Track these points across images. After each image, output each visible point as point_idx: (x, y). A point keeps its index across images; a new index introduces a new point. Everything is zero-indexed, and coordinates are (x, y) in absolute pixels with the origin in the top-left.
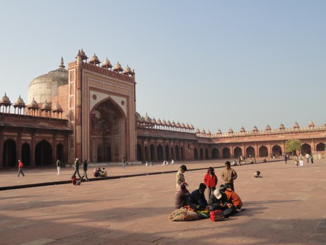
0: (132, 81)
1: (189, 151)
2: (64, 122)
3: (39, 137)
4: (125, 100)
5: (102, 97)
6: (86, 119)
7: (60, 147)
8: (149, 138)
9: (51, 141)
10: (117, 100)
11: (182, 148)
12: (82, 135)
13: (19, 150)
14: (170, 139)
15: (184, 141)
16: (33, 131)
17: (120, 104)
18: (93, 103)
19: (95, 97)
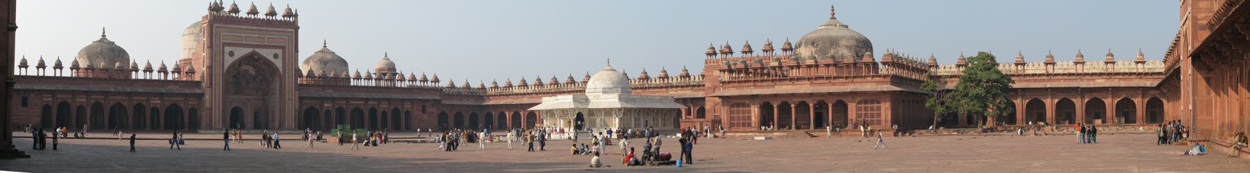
0: (295, 27)
1: (425, 116)
2: (198, 84)
3: (168, 102)
4: (279, 52)
5: (240, 52)
6: (219, 80)
7: (193, 111)
8: (333, 99)
9: (182, 105)
10: (267, 54)
11: (407, 113)
12: (214, 101)
13: (148, 113)
14: (379, 100)
15: (412, 101)
16: (161, 95)
17: (271, 58)
18: (229, 61)
19: (231, 54)
